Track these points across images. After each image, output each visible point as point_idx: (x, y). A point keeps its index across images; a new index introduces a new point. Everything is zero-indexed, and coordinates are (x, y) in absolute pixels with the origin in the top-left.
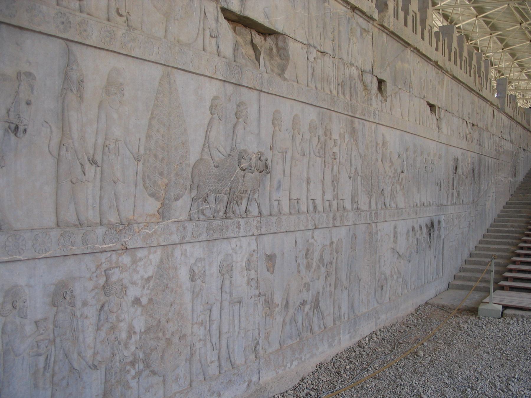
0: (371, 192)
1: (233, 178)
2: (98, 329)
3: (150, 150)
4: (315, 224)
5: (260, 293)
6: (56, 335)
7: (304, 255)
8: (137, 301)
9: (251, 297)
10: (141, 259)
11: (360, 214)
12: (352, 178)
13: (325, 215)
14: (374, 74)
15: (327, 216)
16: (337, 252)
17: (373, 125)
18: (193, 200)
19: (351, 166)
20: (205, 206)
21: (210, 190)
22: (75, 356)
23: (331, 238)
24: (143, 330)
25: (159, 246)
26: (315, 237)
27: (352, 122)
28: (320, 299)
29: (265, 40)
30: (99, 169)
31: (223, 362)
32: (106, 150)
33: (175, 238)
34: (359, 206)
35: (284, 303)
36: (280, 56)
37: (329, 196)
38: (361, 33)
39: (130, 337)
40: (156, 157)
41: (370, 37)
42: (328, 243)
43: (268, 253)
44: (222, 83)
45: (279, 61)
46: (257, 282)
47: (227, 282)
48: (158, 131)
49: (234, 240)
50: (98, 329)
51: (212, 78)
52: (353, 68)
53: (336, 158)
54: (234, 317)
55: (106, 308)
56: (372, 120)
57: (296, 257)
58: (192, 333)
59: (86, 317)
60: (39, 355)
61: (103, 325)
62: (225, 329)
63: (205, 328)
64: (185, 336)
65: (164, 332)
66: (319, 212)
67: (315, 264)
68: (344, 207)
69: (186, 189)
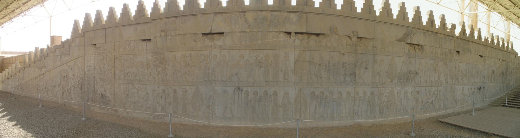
2: (378, 99)
8: (386, 96)
16: (439, 92)
18: (398, 79)
20: (401, 81)
22: (374, 103)
25: (390, 87)
26: (432, 88)
33: (394, 86)
37: (437, 79)
39: (384, 102)
40: (390, 72)
46: (414, 96)
50: (378, 99)
60: (368, 102)
62: (405, 104)
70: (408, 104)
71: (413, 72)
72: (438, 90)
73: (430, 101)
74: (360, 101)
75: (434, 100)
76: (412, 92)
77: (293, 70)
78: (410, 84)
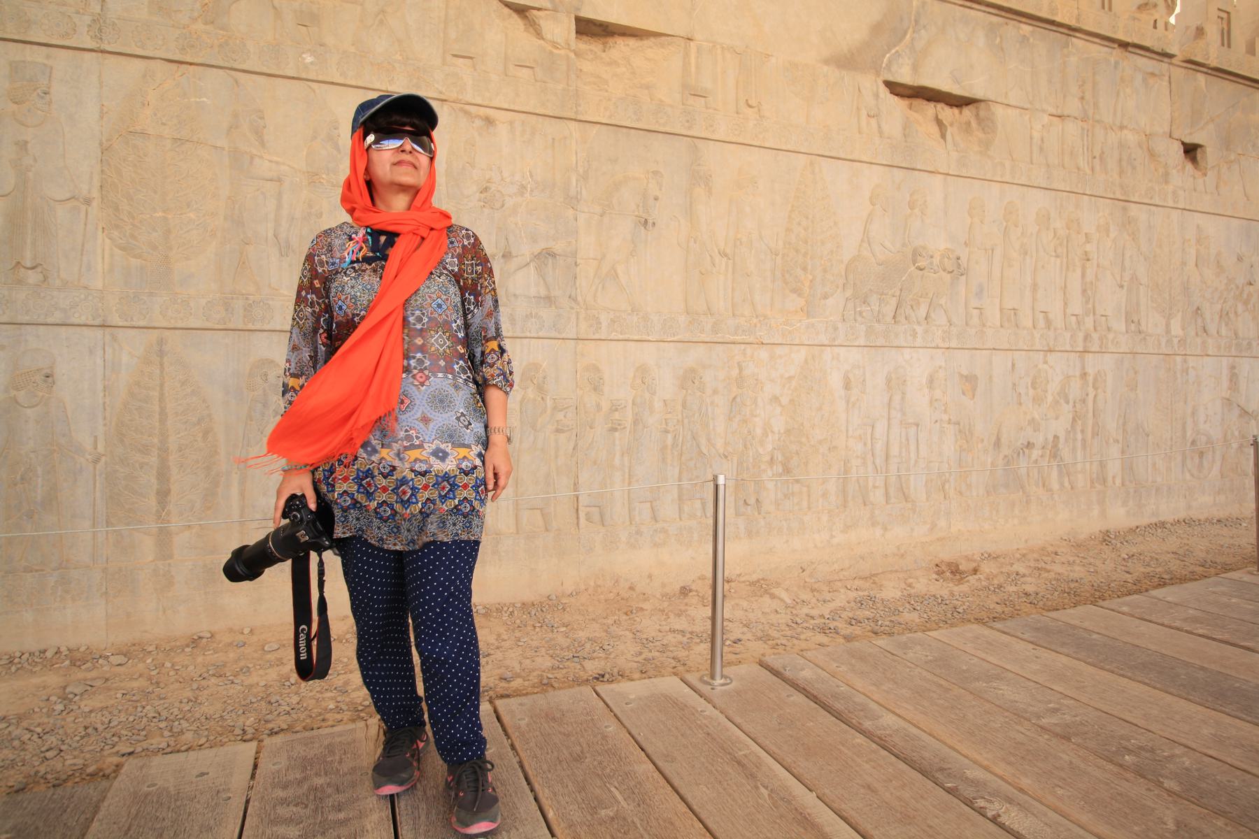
0: (1171, 309)
1: (904, 279)
2: (730, 419)
3: (790, 244)
4: (1048, 344)
5: (950, 419)
6: (684, 415)
7: (1030, 384)
8: (775, 399)
9: (936, 421)
10: (781, 357)
11: (1145, 339)
12: (1125, 288)
13: (1068, 335)
14: (1175, 136)
15: (1072, 336)
16: (1095, 388)
17: (1175, 215)
19: (1123, 269)
20: (864, 308)
21: (871, 290)
22: (703, 441)
23: (1083, 368)
24: (782, 431)
27: (1125, 209)
28: (1060, 446)
29: (961, 113)
30: (731, 262)
31: (892, 491)
32: (738, 243)
33: (823, 339)
34: (1143, 327)
35: (993, 439)
36: (983, 129)
38: (1144, 80)
40: (797, 251)
41: (1165, 83)
42: (1078, 374)
43: (965, 373)
44: (887, 168)
45: (981, 135)
47: (897, 398)
48: (799, 224)
49: (907, 351)
50: (730, 419)
51: (871, 163)
52: (1125, 132)
53: (1091, 258)
54: (907, 440)
55: (738, 400)
56: (1171, 204)
57: (1014, 384)
58: (847, 447)
59: (717, 406)
60: (667, 432)
61: (735, 417)
62: (895, 450)
63: (865, 444)
64: (835, 447)
65: (808, 438)
66: (1055, 329)
67: (1050, 398)
68: (1108, 328)
69: (838, 287)
70: (913, 455)
71: (936, 260)
72: (1084, 375)
73: (1039, 439)
74: (614, 430)
75: (1068, 432)
76: (931, 381)
77: (88, 202)
78: (919, 329)
